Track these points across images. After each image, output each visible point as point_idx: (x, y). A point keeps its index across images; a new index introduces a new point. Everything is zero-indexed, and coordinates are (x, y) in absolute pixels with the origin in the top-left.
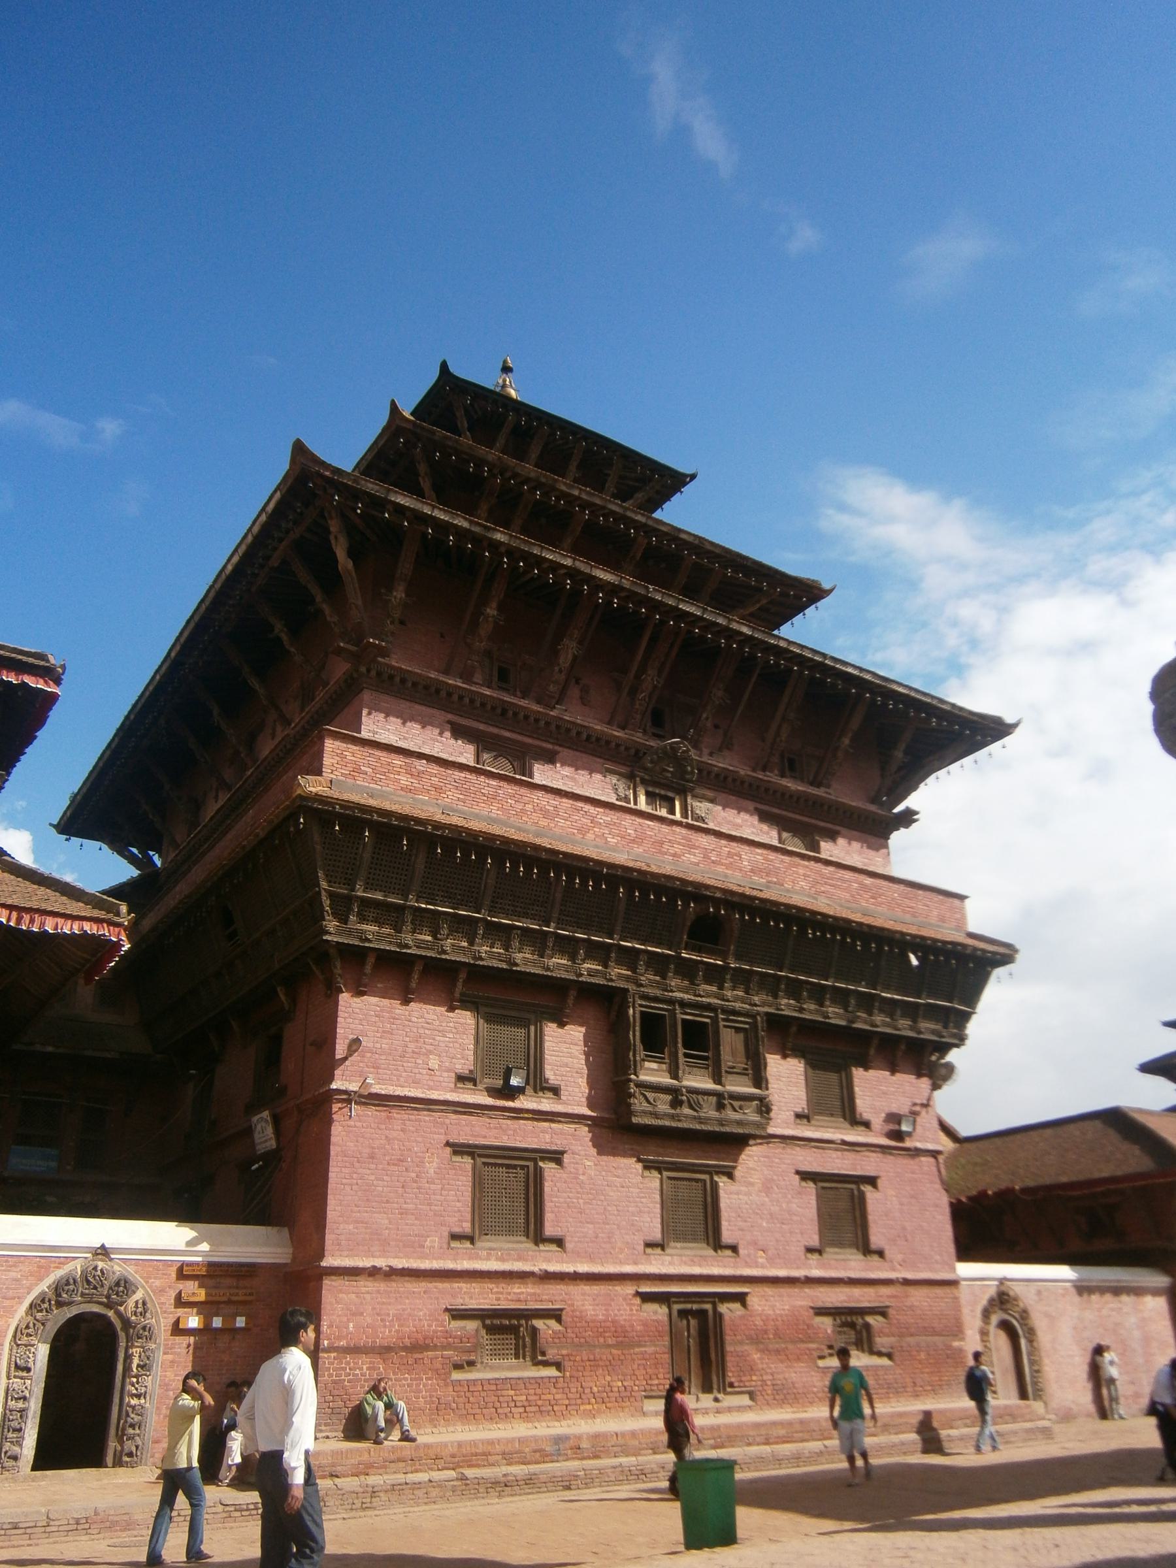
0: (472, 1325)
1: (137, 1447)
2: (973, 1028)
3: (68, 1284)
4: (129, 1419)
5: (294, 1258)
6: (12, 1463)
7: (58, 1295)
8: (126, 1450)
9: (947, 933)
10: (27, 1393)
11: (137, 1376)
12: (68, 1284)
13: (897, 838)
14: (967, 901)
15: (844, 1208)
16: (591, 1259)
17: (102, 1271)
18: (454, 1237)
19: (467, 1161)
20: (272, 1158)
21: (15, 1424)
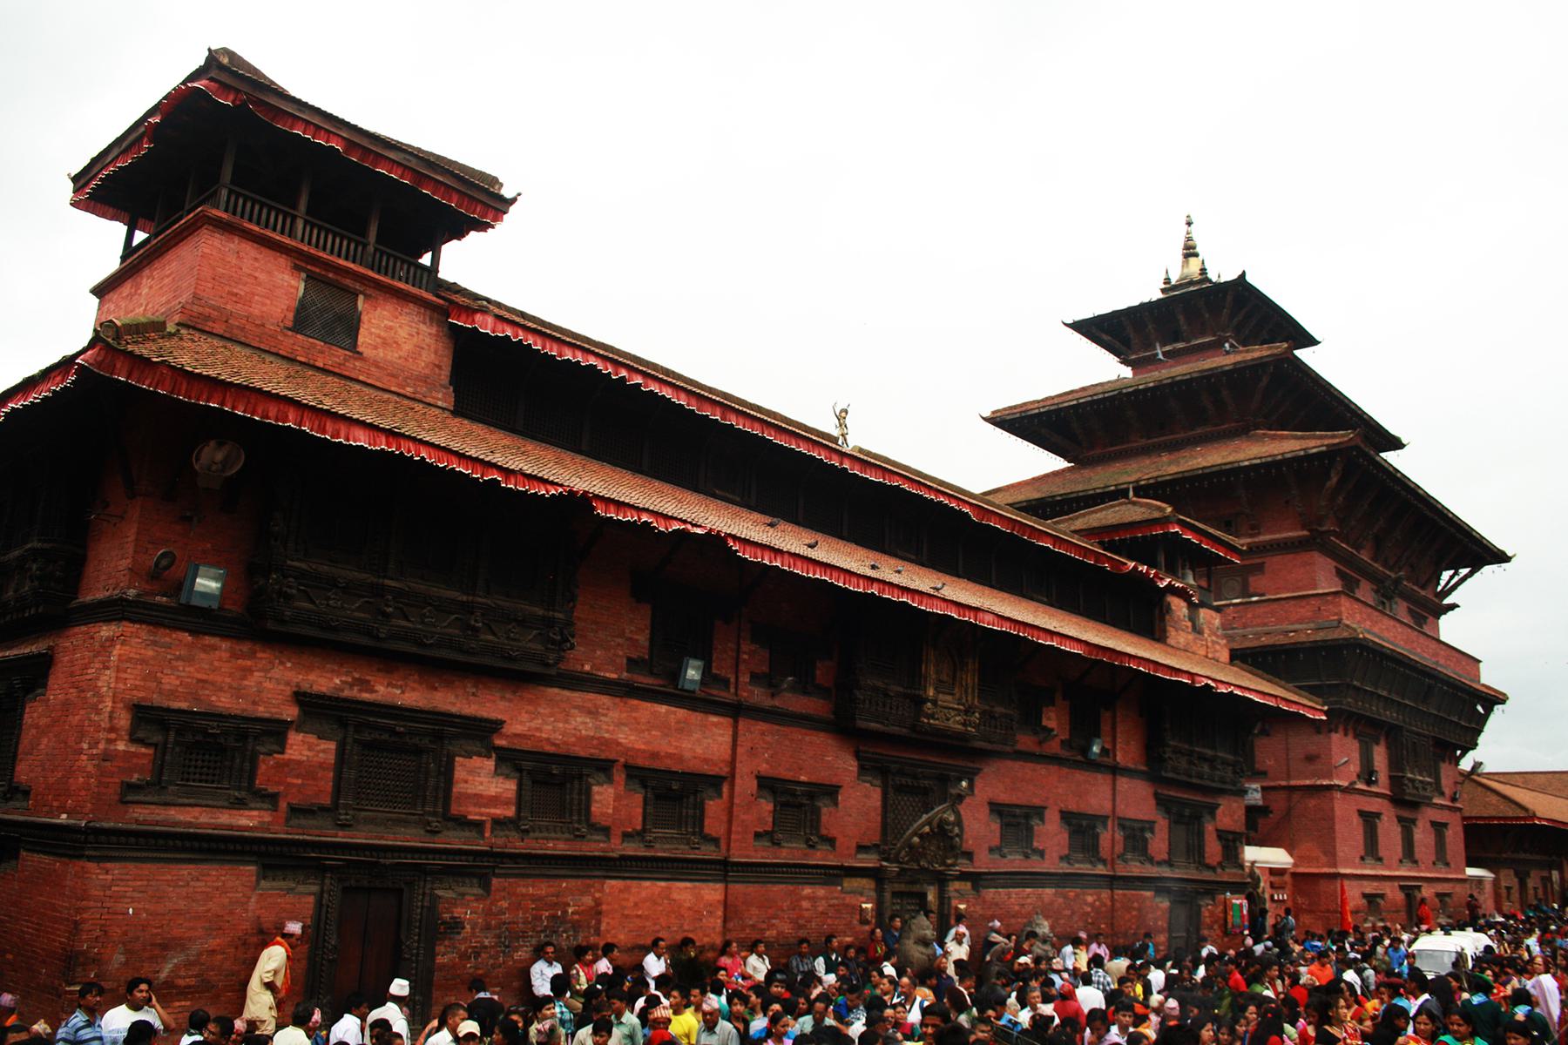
2: (1481, 740)
5: (1295, 865)
16: (1389, 868)
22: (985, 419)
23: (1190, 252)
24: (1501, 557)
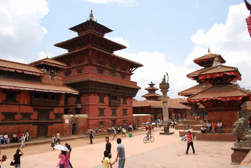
0: (99, 123)
2: (136, 95)
9: (136, 87)
13: (131, 76)
14: (137, 83)
15: (125, 111)
18: (98, 116)
19: (99, 109)
20: (81, 109)
22: (54, 45)
23: (91, 16)
24: (140, 65)
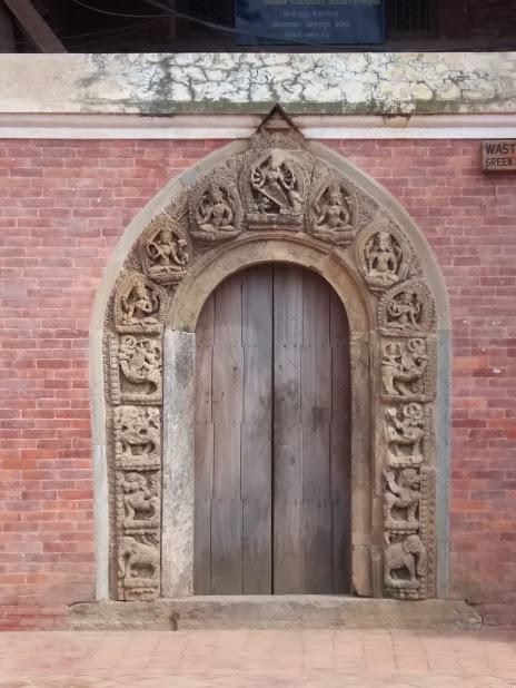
1: (416, 556)
3: (208, 199)
4: (391, 498)
6: (143, 580)
7: (192, 226)
8: (390, 564)
10: (154, 434)
11: (396, 403)
12: (208, 199)
17: (283, 167)
21: (138, 499)
